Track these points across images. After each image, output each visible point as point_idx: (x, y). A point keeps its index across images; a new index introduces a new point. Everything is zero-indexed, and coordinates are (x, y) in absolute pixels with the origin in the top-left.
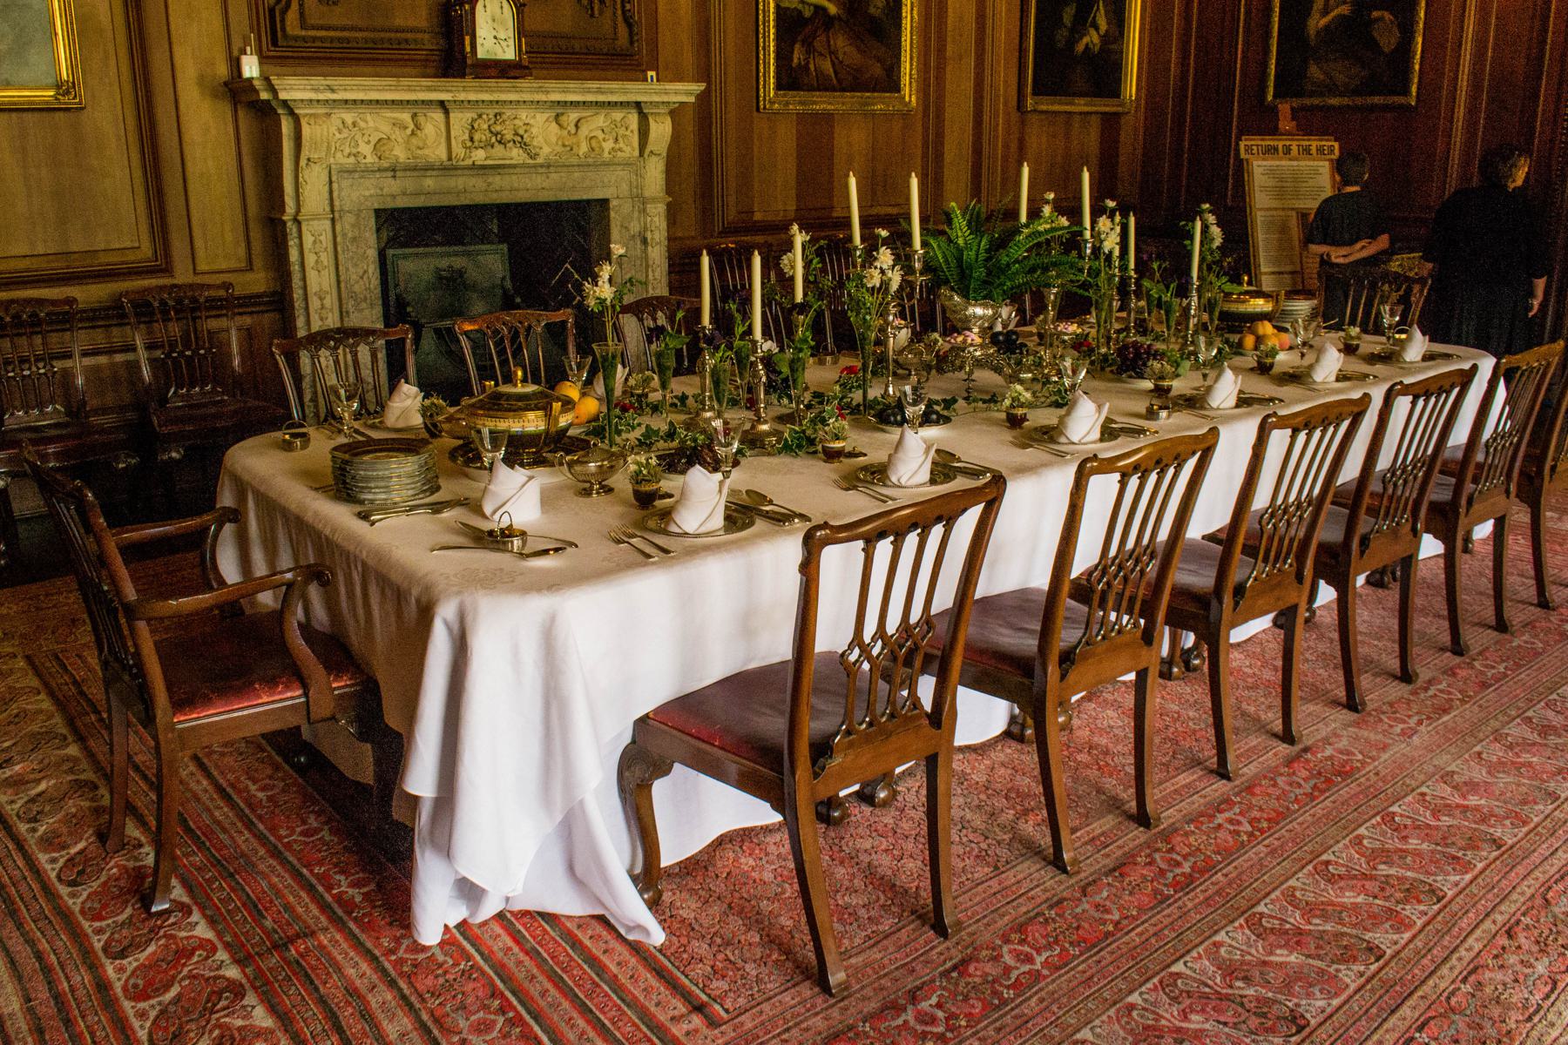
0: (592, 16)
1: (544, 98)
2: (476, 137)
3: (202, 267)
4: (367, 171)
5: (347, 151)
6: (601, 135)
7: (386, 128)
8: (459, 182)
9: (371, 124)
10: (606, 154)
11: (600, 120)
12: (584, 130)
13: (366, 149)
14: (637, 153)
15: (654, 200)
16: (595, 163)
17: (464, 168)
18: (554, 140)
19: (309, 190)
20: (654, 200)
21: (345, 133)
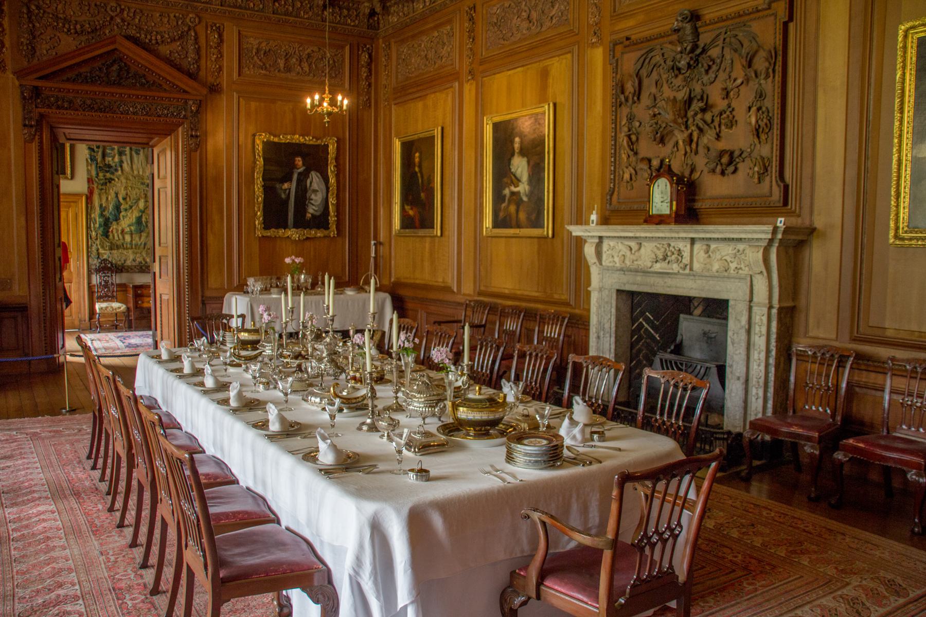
1: (676, 235)
8: (651, 280)
11: (727, 250)
13: (616, 259)
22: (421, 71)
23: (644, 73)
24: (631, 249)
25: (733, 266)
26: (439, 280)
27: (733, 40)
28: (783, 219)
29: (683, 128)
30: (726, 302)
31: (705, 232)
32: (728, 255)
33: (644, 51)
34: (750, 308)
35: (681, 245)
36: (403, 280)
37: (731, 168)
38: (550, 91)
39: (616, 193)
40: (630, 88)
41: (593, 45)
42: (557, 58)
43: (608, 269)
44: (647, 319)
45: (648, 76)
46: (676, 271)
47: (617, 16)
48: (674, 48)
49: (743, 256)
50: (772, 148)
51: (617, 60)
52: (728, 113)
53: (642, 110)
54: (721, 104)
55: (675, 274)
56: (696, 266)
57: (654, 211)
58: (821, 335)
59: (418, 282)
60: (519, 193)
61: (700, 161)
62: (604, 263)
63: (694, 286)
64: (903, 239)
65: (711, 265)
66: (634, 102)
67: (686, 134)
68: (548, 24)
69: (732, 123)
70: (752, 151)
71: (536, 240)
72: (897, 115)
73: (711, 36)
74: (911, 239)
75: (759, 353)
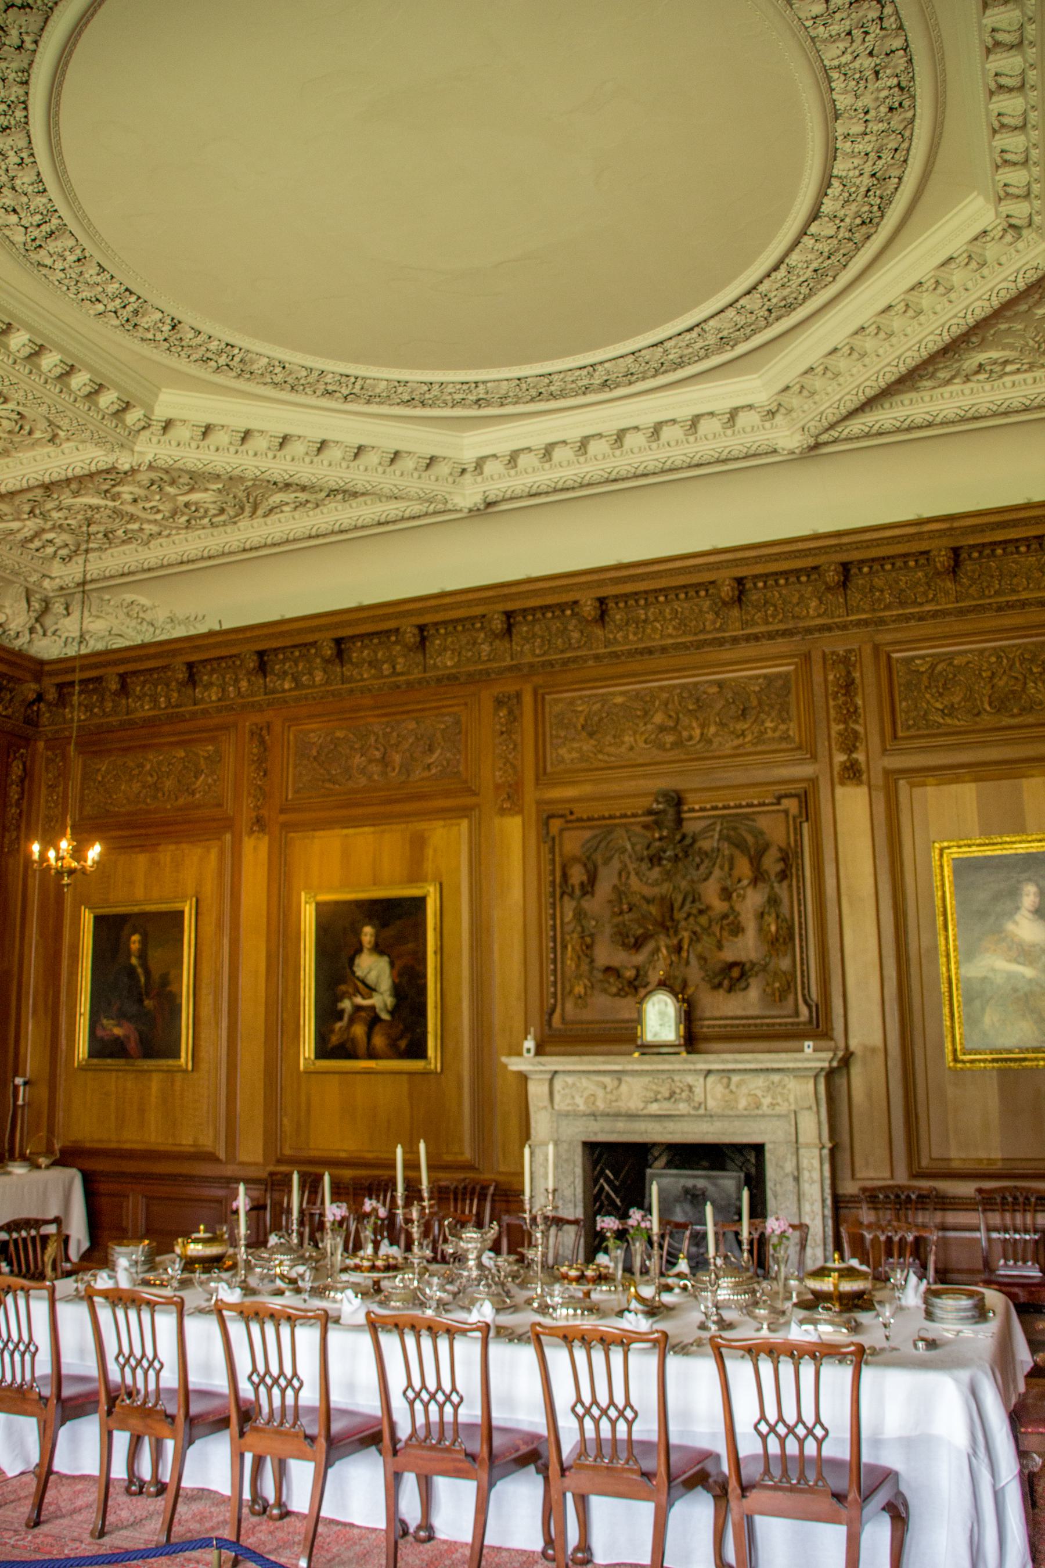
1: (692, 1067)
6: (759, 1093)
10: (765, 1108)
11: (759, 1082)
16: (754, 1113)
17: (645, 1116)
18: (719, 1096)
19: (541, 1124)
21: (567, 1091)
22: (143, 806)
23: (598, 858)
24: (605, 1087)
25: (766, 1101)
26: (186, 1140)
27: (732, 833)
28: (811, 1043)
29: (671, 932)
31: (736, 1061)
32: (757, 1088)
33: (597, 832)
34: (797, 1149)
35: (690, 1079)
36: (88, 1145)
37: (743, 984)
38: (429, 867)
39: (558, 1010)
40: (578, 876)
41: (502, 812)
42: (441, 823)
43: (567, 1115)
44: (608, 1180)
45: (607, 861)
46: (685, 1112)
47: (542, 777)
48: (648, 834)
49: (779, 1089)
51: (553, 839)
52: (731, 918)
53: (597, 904)
55: (682, 1116)
56: (711, 1103)
57: (649, 1037)
58: (872, 1174)
59: (128, 1146)
60: (373, 1008)
61: (694, 973)
62: (556, 1107)
63: (711, 1129)
64: (963, 1062)
65: (737, 1101)
66: (584, 893)
67: (675, 941)
68: (418, 774)
70: (767, 965)
71: (405, 1077)
72: (942, 932)
73: (702, 824)
74: (972, 1061)
75: (812, 1204)
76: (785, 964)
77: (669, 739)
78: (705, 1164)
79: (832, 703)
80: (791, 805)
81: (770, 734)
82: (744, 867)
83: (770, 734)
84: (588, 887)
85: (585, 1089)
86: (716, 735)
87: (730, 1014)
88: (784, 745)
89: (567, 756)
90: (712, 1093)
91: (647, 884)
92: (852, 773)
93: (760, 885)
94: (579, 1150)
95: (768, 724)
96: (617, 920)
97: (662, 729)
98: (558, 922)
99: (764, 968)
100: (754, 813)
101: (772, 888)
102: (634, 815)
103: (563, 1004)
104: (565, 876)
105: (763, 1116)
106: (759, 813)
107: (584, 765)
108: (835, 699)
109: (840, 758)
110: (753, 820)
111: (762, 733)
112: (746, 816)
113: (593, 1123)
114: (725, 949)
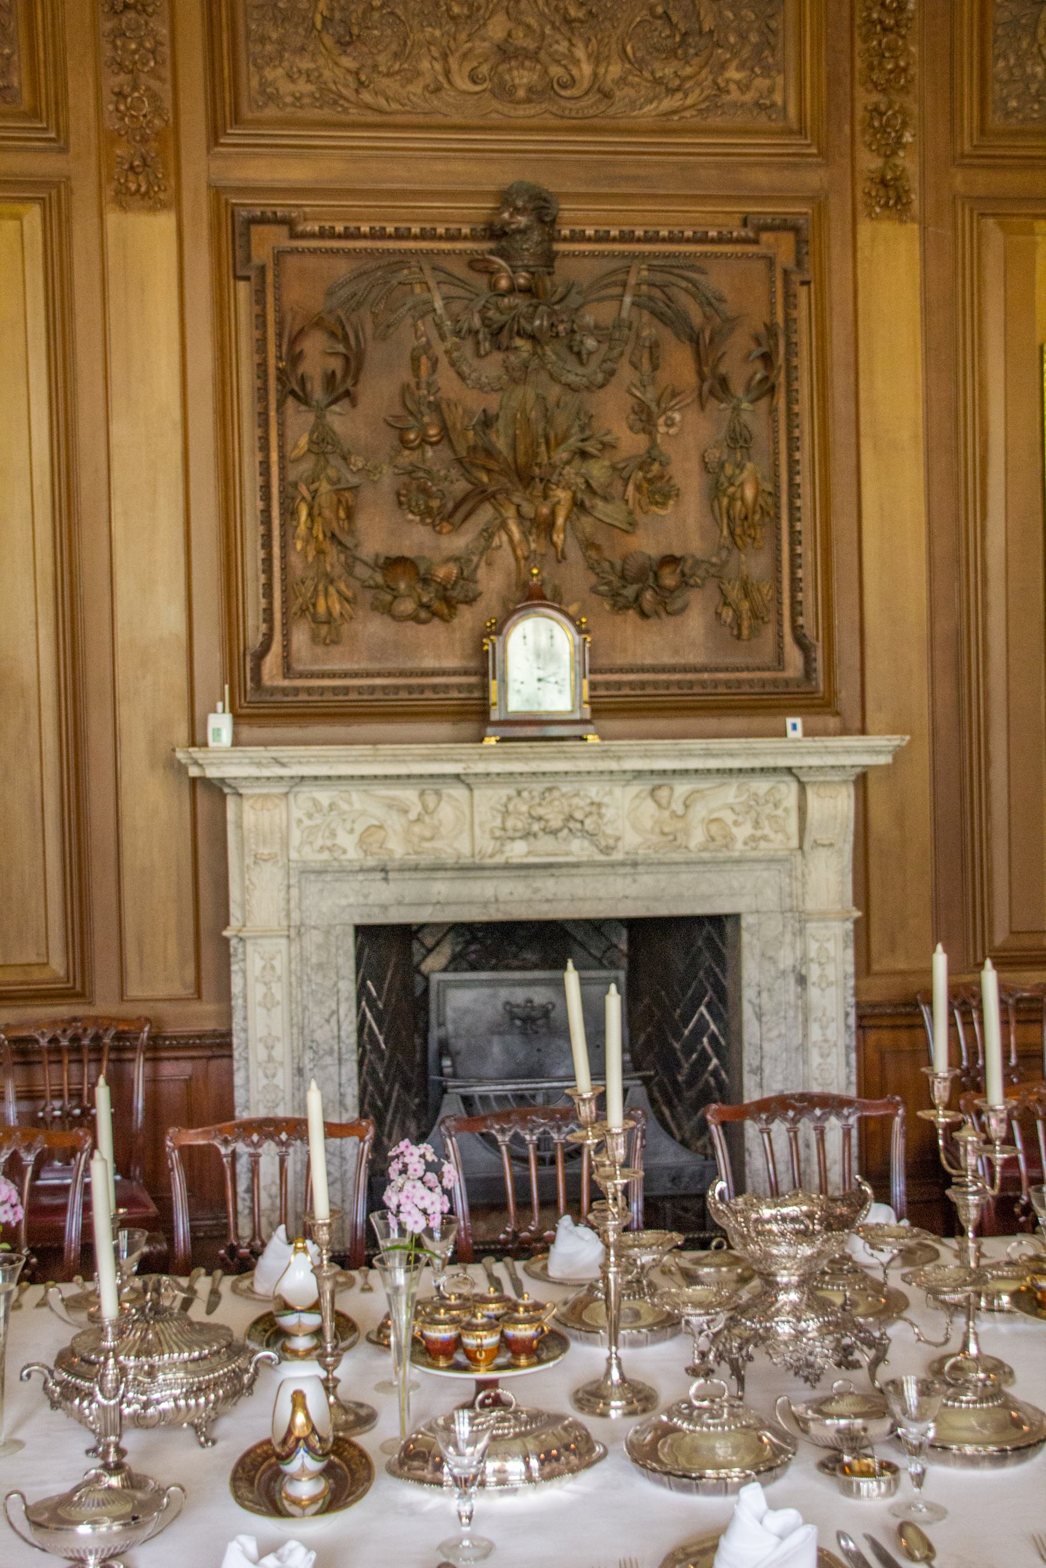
0: (739, 637)
1: (614, 766)
2: (510, 824)
3: (134, 991)
4: (345, 872)
5: (319, 842)
6: (729, 817)
7: (377, 812)
9: (357, 806)
10: (739, 845)
11: (731, 793)
12: (699, 811)
13: (348, 842)
14: (794, 843)
15: (823, 916)
16: (718, 859)
17: (496, 868)
18: (648, 824)
19: (258, 899)
20: (823, 916)
21: (318, 820)
25: (742, 833)
27: (657, 293)
28: (798, 721)
30: (736, 917)
31: (709, 754)
39: (276, 647)
40: (318, 357)
49: (768, 809)
50: (778, 560)
51: (262, 270)
54: (631, 443)
57: (516, 703)
63: (632, 890)
65: (687, 833)
69: (660, 491)
76: (755, 564)
77: (523, 77)
78: (530, 956)
79: (859, 45)
80: (783, 247)
81: (735, 95)
82: (680, 365)
83: (735, 95)
84: (342, 389)
85: (364, 813)
86: (622, 81)
87: (649, 661)
88: (762, 121)
89: (286, 88)
90: (627, 816)
91: (473, 385)
92: (891, 195)
93: (712, 404)
94: (349, 944)
95: (733, 74)
96: (407, 457)
97: (505, 52)
98: (274, 456)
99: (718, 573)
100: (705, 255)
101: (736, 409)
102: (450, 237)
103: (286, 636)
104: (296, 358)
105: (738, 861)
106: (717, 256)
107: (326, 113)
108: (866, 39)
109: (870, 162)
110: (703, 272)
111: (721, 91)
112: (691, 264)
113: (383, 885)
114: (640, 532)
